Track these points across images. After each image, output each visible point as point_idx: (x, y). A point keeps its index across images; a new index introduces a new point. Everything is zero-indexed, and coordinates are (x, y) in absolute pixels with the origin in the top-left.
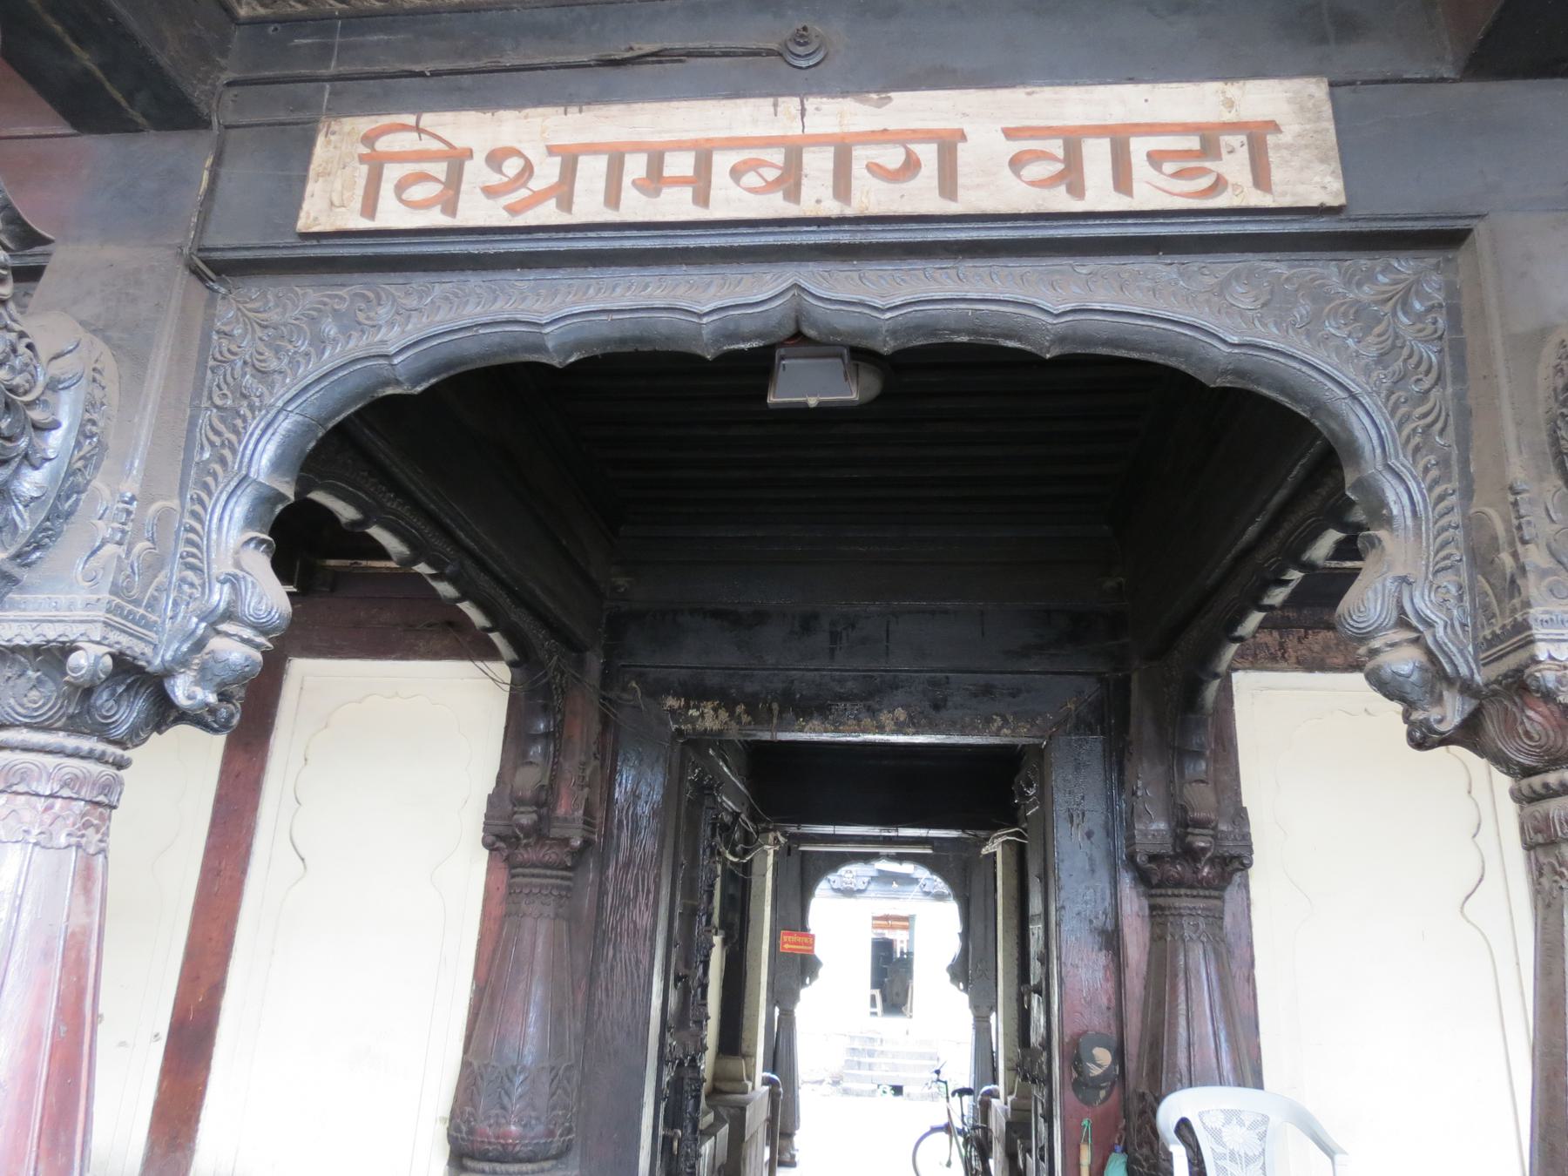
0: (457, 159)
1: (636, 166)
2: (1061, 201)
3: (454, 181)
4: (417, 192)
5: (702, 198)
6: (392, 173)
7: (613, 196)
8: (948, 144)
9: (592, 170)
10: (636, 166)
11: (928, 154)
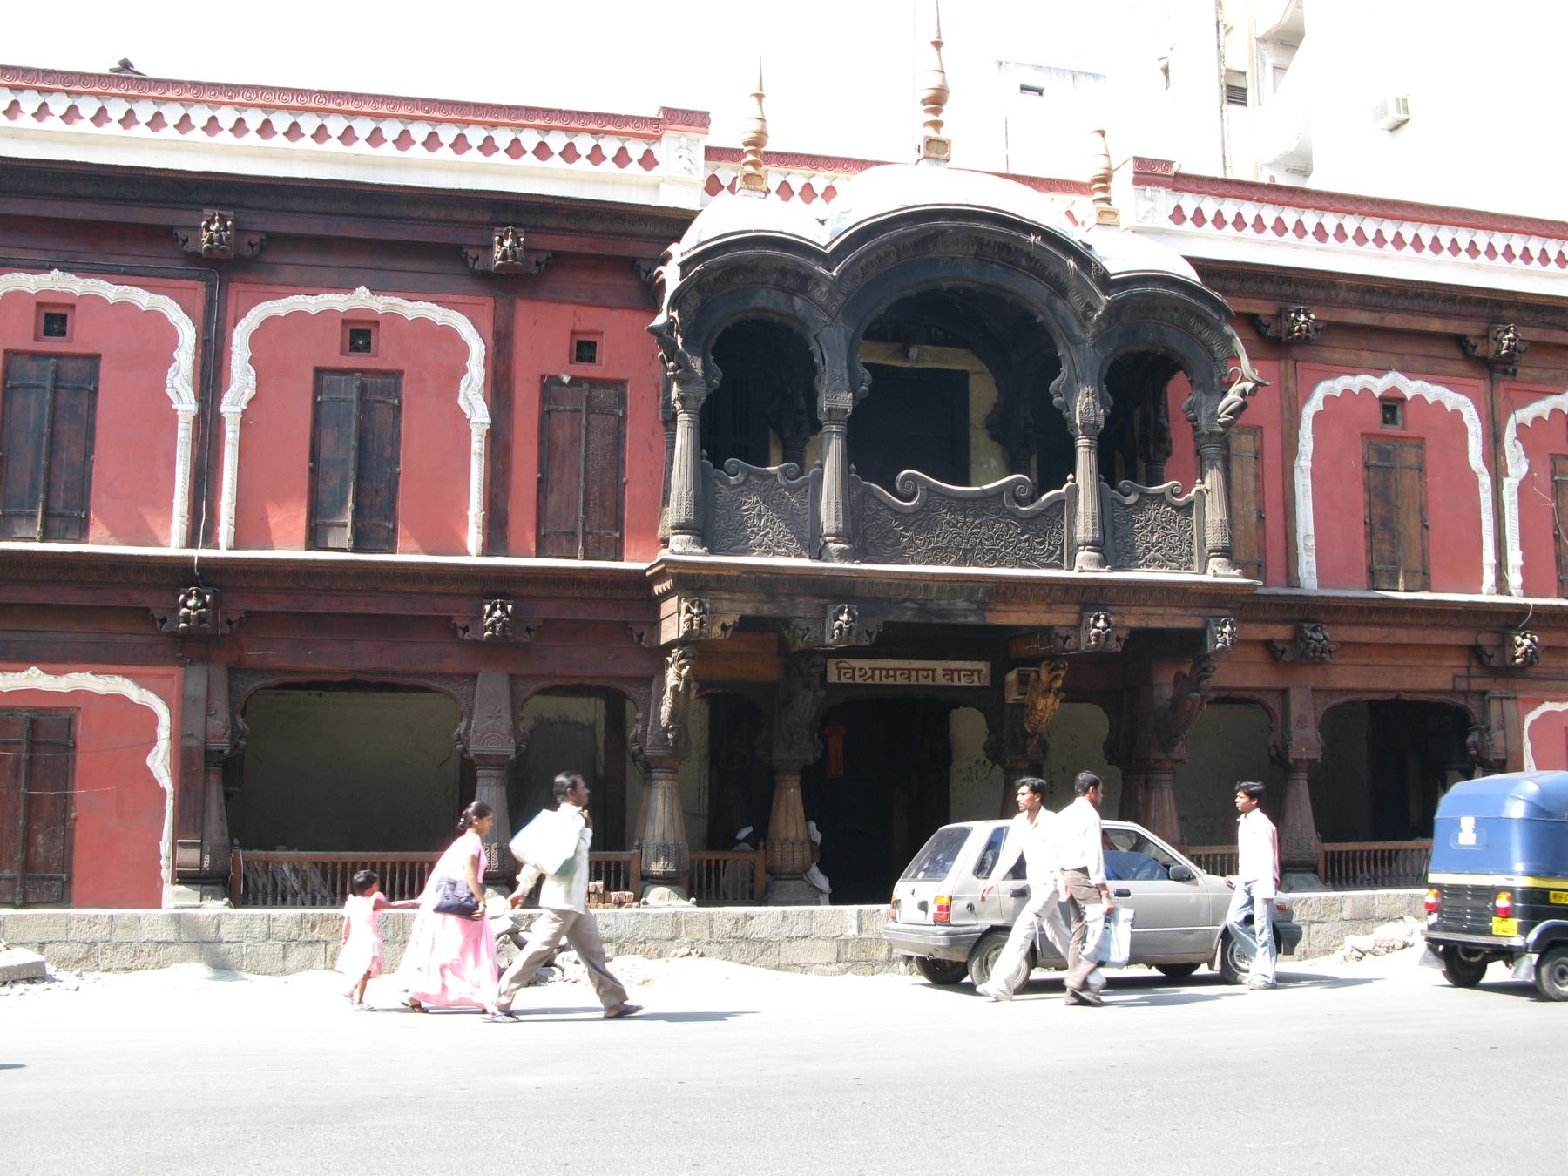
0: (854, 669)
1: (884, 673)
2: (950, 683)
3: (854, 674)
4: (848, 676)
5: (895, 680)
6: (843, 671)
7: (881, 679)
8: (934, 671)
9: (877, 673)
10: (884, 673)
11: (930, 673)
